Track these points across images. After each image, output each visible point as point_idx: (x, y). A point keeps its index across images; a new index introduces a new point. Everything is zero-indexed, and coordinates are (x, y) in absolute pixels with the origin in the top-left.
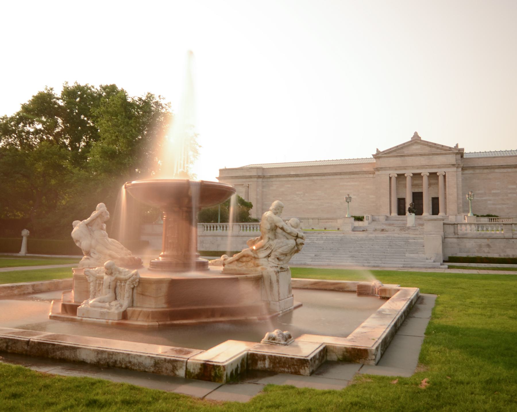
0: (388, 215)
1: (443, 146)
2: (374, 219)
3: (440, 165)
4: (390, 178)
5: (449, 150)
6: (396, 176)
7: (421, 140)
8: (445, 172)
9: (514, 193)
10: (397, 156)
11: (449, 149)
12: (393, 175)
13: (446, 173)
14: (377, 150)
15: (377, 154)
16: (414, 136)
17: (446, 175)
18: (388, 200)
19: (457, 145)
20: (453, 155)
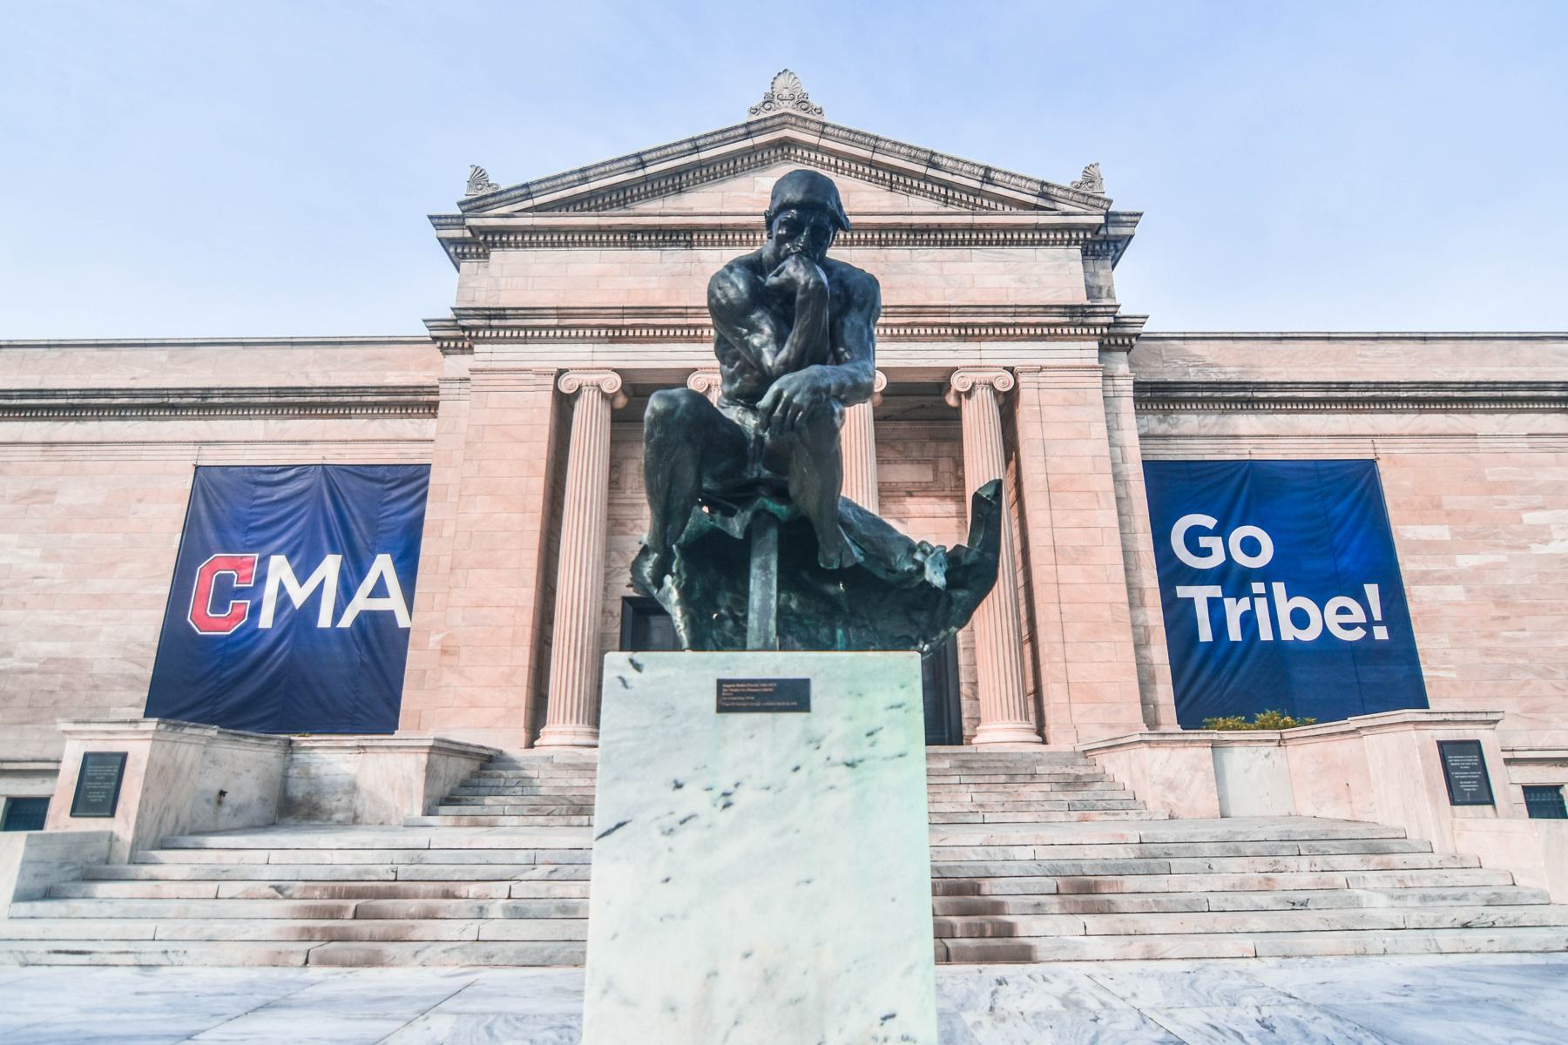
0: (507, 738)
1: (987, 176)
2: (298, 790)
3: (980, 309)
4: (564, 405)
5: (1036, 207)
6: (613, 383)
7: (823, 129)
8: (1011, 370)
9: (1446, 579)
10: (633, 237)
11: (1033, 200)
12: (594, 378)
13: (1022, 379)
14: (479, 177)
15: (474, 206)
16: (769, 100)
17: (1026, 395)
18: (527, 595)
19: (1090, 178)
20: (1059, 251)
